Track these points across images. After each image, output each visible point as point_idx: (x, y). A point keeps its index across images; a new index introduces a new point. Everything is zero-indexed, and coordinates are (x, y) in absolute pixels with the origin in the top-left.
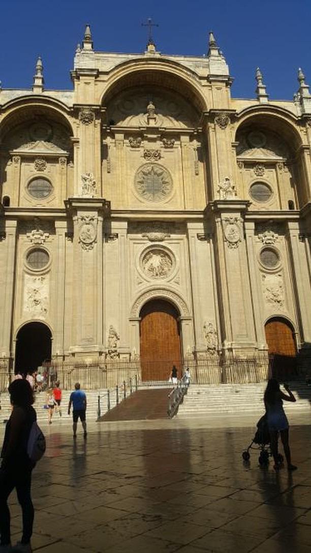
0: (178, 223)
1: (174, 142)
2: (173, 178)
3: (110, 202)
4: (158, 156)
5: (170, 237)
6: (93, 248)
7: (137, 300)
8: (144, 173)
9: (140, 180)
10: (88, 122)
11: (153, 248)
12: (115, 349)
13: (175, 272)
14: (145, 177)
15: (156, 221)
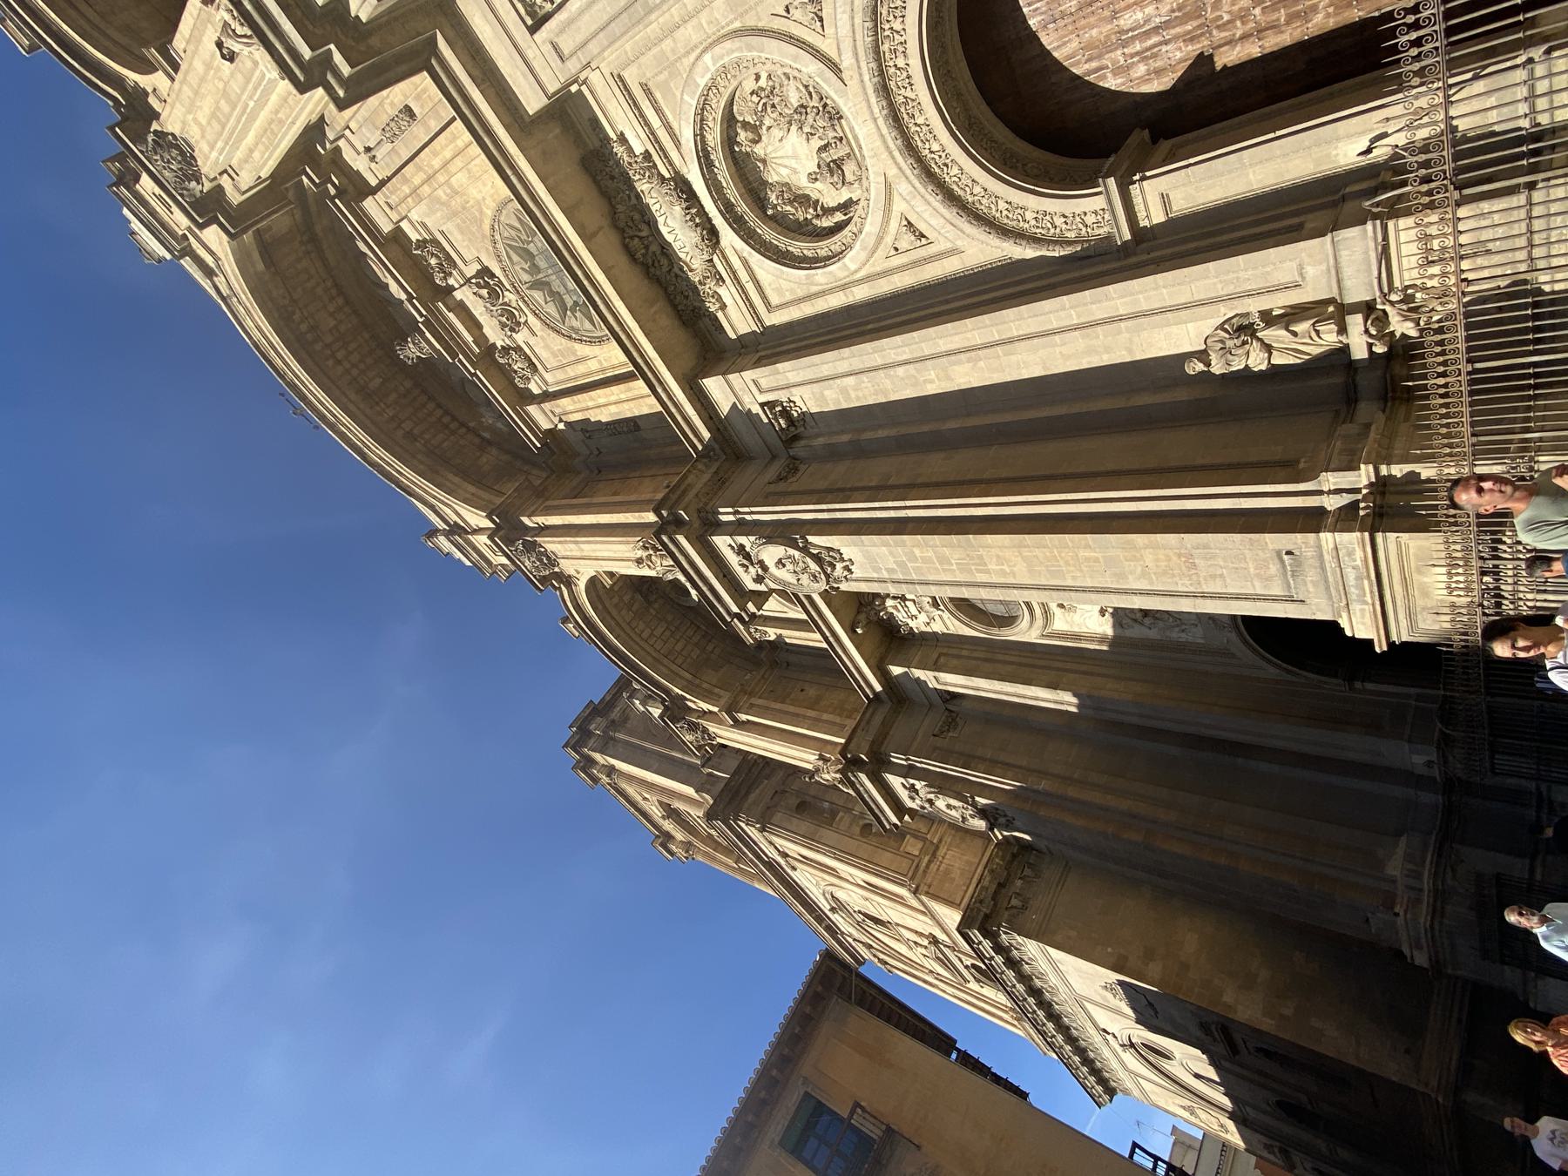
0: (578, 140)
1: (422, 244)
2: (493, 205)
3: (657, 511)
4: (487, 285)
5: (647, 156)
6: (830, 549)
7: (1004, 232)
8: (563, 309)
9: (588, 325)
10: (545, 553)
11: (742, 207)
12: (1356, 322)
13: (776, 51)
14: (569, 303)
15: (631, 255)
